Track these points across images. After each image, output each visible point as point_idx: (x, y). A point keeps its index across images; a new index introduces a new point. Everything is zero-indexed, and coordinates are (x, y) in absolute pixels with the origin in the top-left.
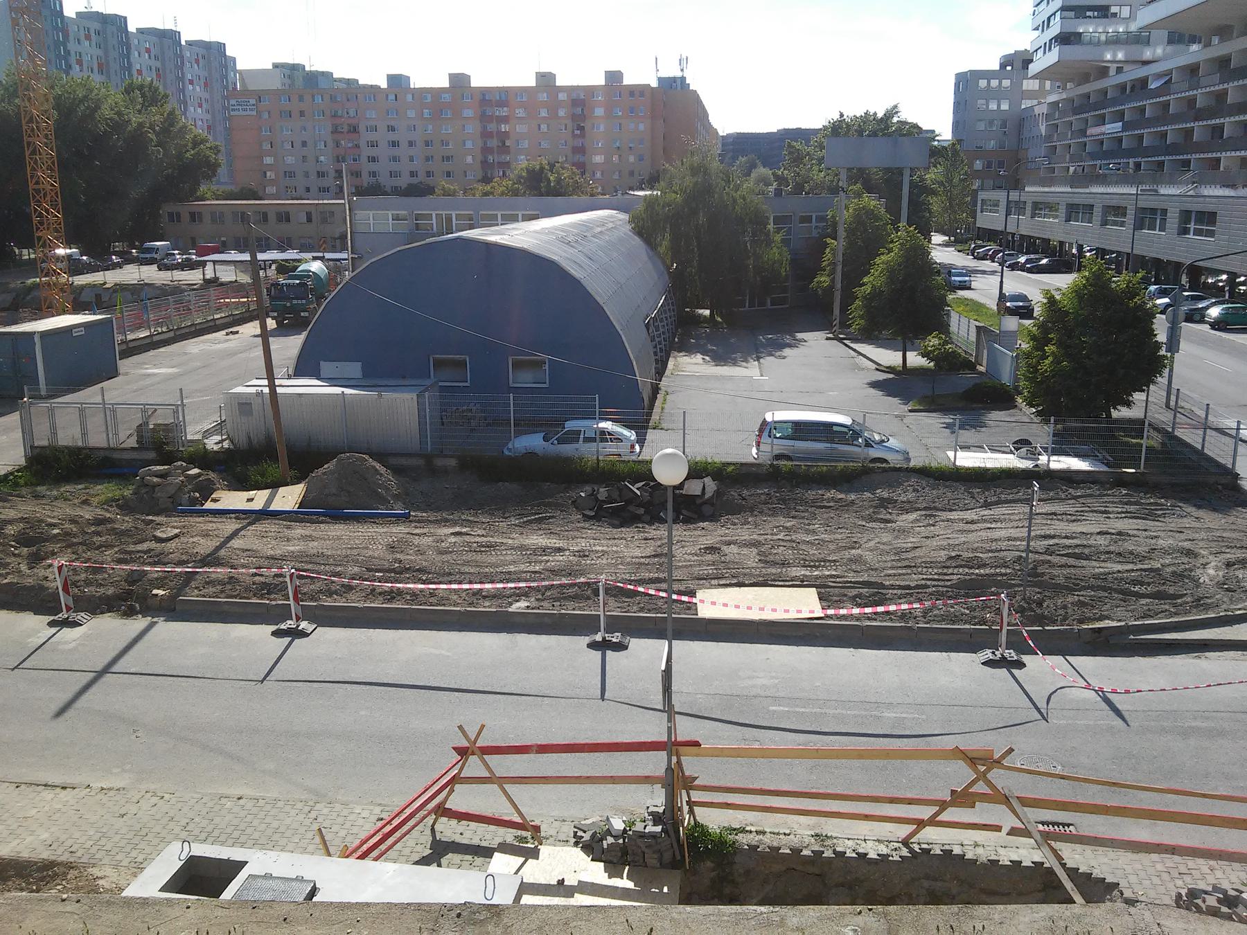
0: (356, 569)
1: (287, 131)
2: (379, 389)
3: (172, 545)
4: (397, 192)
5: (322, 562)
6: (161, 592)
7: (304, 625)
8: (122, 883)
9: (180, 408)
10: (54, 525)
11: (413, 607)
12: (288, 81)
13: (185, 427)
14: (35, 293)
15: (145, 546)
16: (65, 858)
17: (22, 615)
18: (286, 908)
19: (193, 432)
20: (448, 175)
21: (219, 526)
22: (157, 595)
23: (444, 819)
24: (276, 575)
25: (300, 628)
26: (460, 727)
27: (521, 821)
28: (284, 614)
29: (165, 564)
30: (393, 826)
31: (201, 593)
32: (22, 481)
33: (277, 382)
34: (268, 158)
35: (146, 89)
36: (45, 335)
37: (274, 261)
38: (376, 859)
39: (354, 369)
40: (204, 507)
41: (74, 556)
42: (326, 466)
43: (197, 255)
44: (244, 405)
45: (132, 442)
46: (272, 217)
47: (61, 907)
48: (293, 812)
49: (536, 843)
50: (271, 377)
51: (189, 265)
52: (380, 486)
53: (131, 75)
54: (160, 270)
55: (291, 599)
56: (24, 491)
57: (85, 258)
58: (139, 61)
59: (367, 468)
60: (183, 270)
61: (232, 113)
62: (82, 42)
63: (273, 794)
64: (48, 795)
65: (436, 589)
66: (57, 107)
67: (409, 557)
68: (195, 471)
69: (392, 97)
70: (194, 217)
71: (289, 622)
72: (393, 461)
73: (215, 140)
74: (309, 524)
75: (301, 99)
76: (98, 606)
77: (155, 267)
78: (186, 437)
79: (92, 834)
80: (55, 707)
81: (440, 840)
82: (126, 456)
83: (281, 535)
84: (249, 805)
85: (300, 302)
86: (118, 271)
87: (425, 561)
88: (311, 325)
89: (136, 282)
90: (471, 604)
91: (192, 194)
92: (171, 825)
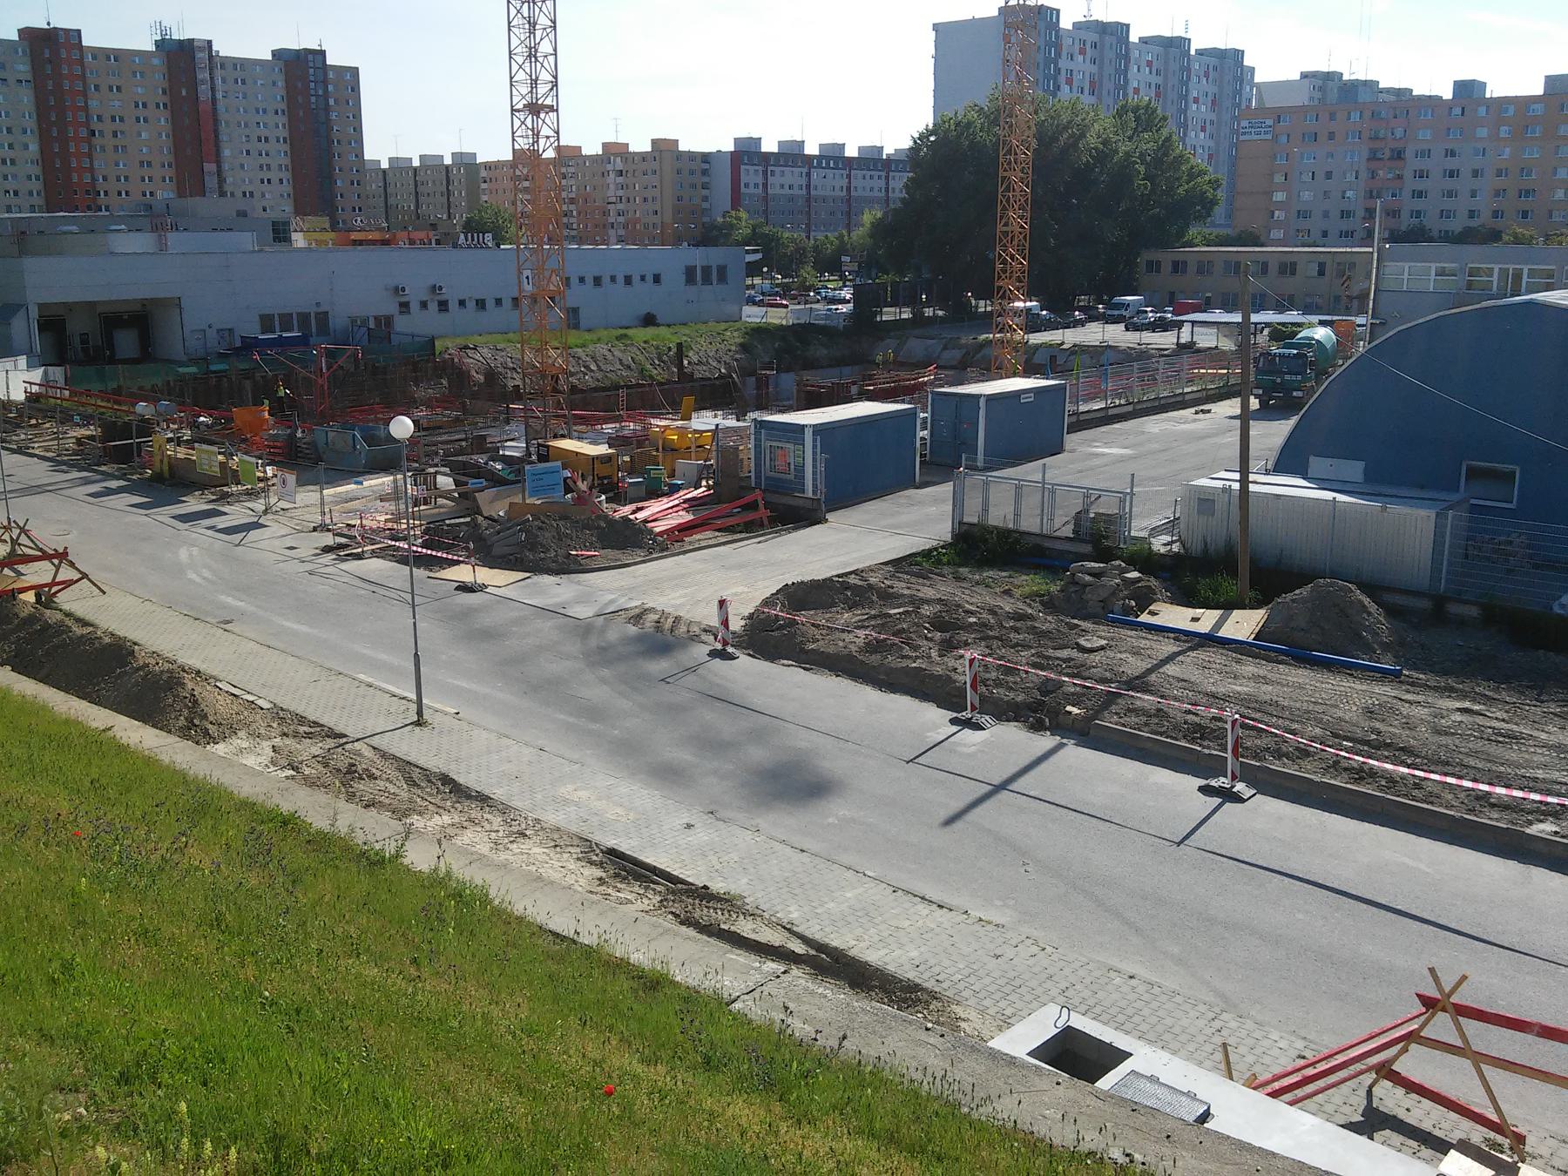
0: (1318, 730)
1: (1308, 159)
2: (1386, 499)
3: (1096, 658)
4: (1449, 238)
5: (1275, 713)
6: (1075, 710)
7: (1240, 787)
8: (986, 1033)
9: (1128, 497)
10: (972, 613)
11: (1389, 797)
12: (1318, 95)
13: (1131, 520)
14: (985, 351)
15: (1065, 653)
16: (929, 985)
17: (926, 705)
18: (1170, 1125)
19: (1139, 528)
20: (1525, 215)
21: (1153, 643)
22: (1070, 713)
23: (1387, 1084)
24: (1214, 718)
25: (1234, 790)
26: (1432, 970)
27: (1498, 1121)
28: (1217, 767)
29: (1085, 679)
30: (1316, 1071)
31: (1121, 720)
32: (945, 559)
33: (1252, 477)
34: (1280, 194)
35: (1142, 111)
36: (991, 398)
37: (1267, 325)
38: (1292, 1103)
39: (1354, 470)
40: (1138, 620)
41: (988, 651)
42: (1297, 592)
43: (1174, 313)
44: (1205, 502)
45: (1068, 531)
46: (1273, 268)
47: (923, 1035)
48: (1193, 1014)
49: (1516, 1158)
50: (1244, 471)
51: (1161, 326)
52: (1366, 629)
53: (1125, 95)
54: (1127, 330)
55: (1230, 751)
56: (946, 570)
57: (1044, 313)
58: (1138, 77)
59: (1352, 602)
60: (1154, 332)
61: (1242, 138)
62: (1075, 58)
63: (1170, 984)
64: (923, 909)
65: (1425, 778)
66: (1040, 136)
67: (1392, 729)
68: (1135, 575)
69: (1458, 111)
70: (1178, 267)
71: (1222, 779)
72: (1389, 598)
73: (1216, 172)
74: (1264, 662)
75: (1332, 116)
76: (1006, 712)
77: (1122, 326)
78: (1129, 532)
79: (961, 966)
80: (944, 814)
81: (1377, 1109)
82: (1058, 546)
83: (1228, 669)
84: (1142, 988)
85: (1294, 378)
86: (1079, 330)
87: (1414, 738)
88: (1303, 411)
89: (1098, 343)
90: (1471, 811)
91: (1179, 238)
92: (1049, 984)
